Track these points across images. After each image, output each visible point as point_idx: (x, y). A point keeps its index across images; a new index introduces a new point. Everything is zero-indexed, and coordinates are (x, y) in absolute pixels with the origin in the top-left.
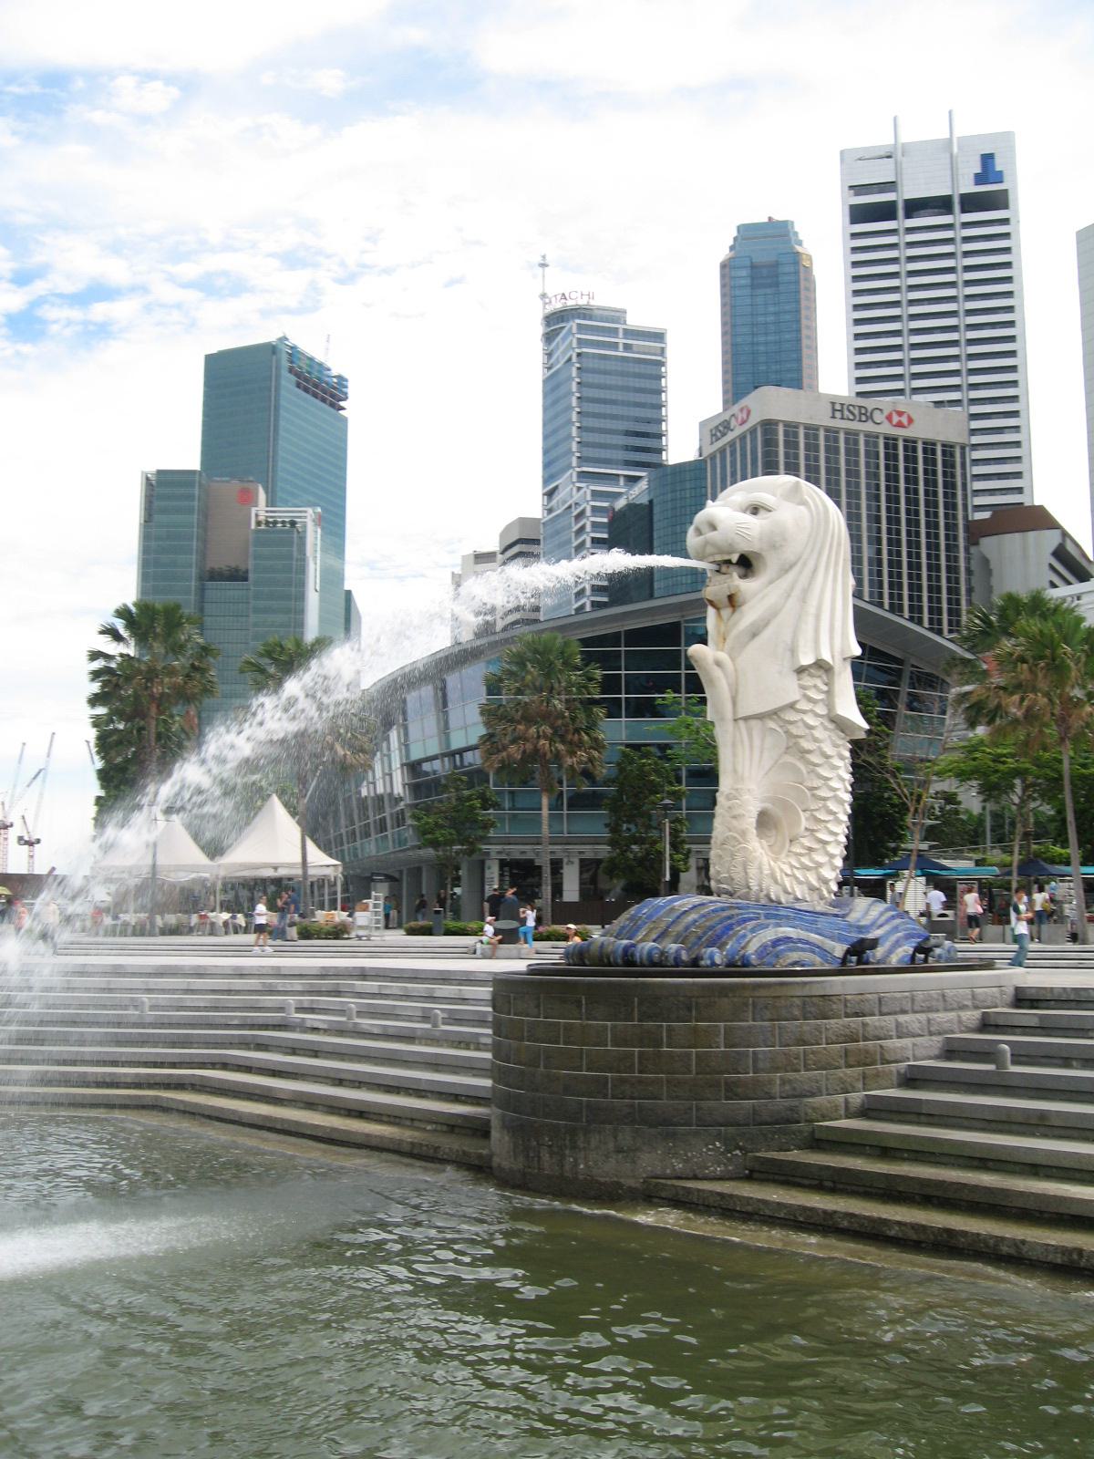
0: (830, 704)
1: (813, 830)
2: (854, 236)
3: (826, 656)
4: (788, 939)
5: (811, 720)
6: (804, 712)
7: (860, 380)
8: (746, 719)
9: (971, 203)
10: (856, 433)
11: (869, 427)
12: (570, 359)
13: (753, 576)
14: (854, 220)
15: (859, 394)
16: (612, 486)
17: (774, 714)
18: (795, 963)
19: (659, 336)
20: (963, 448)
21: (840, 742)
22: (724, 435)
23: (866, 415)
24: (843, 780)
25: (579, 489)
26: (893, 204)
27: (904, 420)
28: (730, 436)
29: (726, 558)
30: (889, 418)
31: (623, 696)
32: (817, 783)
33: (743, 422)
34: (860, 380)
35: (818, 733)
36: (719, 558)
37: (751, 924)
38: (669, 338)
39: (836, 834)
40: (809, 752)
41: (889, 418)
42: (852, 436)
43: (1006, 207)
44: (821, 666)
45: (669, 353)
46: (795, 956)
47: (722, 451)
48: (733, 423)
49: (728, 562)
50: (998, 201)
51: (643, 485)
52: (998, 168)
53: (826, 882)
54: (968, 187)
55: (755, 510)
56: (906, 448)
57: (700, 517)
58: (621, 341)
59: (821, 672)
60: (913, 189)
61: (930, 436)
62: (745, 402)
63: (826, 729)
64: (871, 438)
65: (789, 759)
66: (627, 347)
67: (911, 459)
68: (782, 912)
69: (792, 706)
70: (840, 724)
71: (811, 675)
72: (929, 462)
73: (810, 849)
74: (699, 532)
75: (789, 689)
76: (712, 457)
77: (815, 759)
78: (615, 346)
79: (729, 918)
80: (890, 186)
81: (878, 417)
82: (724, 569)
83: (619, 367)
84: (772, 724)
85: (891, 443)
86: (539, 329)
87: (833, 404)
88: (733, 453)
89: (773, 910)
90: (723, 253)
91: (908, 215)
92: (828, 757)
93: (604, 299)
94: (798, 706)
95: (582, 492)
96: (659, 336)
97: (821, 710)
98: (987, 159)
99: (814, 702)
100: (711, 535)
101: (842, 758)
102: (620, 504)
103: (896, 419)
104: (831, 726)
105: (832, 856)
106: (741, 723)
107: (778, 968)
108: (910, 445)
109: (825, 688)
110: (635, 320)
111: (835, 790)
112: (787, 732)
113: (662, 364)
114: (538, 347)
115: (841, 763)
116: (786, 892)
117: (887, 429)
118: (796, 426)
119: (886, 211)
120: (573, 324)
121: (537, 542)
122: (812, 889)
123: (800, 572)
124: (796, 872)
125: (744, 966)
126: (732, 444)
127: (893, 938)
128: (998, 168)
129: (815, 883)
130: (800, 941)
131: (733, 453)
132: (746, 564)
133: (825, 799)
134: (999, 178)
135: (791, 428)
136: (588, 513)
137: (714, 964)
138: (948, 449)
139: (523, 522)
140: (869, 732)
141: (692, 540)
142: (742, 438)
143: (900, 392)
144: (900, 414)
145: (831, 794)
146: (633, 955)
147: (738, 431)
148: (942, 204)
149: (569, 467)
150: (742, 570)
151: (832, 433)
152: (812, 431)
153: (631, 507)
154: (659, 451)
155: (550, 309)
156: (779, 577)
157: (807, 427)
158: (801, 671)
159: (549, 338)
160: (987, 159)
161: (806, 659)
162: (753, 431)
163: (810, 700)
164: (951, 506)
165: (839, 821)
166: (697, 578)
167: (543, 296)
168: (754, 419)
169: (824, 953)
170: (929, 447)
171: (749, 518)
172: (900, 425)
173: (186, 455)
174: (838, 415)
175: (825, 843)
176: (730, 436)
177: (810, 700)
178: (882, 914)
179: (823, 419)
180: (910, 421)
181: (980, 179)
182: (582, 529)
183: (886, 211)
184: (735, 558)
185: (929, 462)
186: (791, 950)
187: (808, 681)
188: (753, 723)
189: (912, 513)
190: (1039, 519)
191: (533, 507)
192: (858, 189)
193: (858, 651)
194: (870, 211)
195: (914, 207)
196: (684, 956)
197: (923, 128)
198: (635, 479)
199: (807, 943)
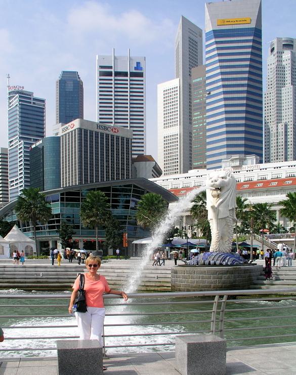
9: (133, 74)
11: (107, 132)
14: (100, 76)
15: (100, 122)
19: (43, 101)
20: (131, 139)
23: (106, 128)
25: (20, 141)
30: (112, 130)
33: (72, 128)
34: (100, 118)
38: (46, 102)
41: (112, 130)
42: (102, 134)
45: (46, 106)
47: (66, 135)
48: (69, 127)
50: (141, 75)
51: (41, 142)
56: (121, 139)
58: (32, 101)
62: (72, 122)
66: (34, 103)
72: (122, 143)
76: (62, 136)
78: (30, 103)
80: (111, 67)
85: (112, 136)
88: (69, 136)
90: (57, 77)
95: (21, 142)
98: (138, 64)
102: (33, 146)
108: (118, 138)
110: (36, 96)
113: (43, 109)
117: (111, 133)
119: (110, 74)
126: (69, 133)
131: (69, 136)
134: (141, 69)
135: (86, 131)
138: (128, 140)
142: (72, 132)
144: (115, 129)
147: (70, 130)
148: (125, 74)
151: (97, 133)
152: (91, 132)
153: (36, 147)
160: (138, 64)
162: (75, 130)
164: (127, 153)
170: (123, 139)
172: (115, 132)
180: (118, 131)
181: (136, 68)
183: (110, 74)
185: (122, 143)
190: (149, 159)
192: (101, 67)
194: (105, 73)
195: (117, 74)
198: (37, 140)
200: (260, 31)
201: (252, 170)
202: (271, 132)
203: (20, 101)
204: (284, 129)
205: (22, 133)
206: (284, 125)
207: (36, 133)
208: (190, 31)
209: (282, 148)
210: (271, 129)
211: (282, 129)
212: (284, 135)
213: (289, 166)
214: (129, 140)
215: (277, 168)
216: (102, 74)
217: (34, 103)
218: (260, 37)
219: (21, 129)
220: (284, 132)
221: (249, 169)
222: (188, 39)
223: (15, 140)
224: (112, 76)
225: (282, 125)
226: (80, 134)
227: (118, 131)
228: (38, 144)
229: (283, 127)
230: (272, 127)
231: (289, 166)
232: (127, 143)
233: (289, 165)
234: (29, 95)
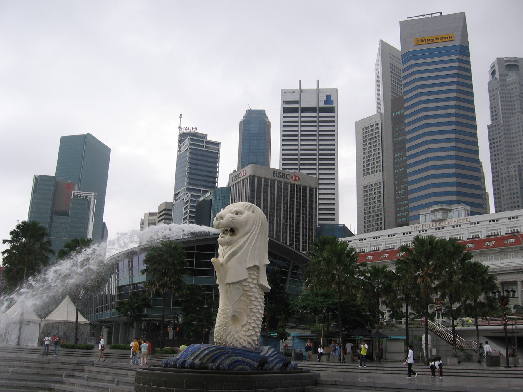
0: (258, 281)
1: (250, 323)
2: (284, 117)
3: (257, 263)
4: (238, 361)
5: (252, 286)
6: (250, 282)
7: (283, 164)
8: (229, 284)
9: (322, 110)
10: (281, 182)
11: (285, 180)
12: (187, 149)
13: (235, 235)
14: (284, 113)
16: (198, 193)
17: (239, 282)
18: (241, 369)
19: (218, 144)
21: (261, 293)
22: (237, 179)
23: (285, 176)
24: (262, 306)
25: (187, 193)
26: (298, 108)
27: (297, 179)
28: (239, 180)
29: (226, 229)
30: (292, 178)
31: (194, 268)
32: (253, 307)
34: (283, 164)
35: (255, 290)
36: (223, 229)
37: (226, 356)
38: (221, 145)
39: (258, 325)
40: (250, 296)
41: (292, 178)
42: (279, 183)
43: (334, 112)
44: (256, 267)
46: (240, 367)
47: (236, 184)
49: (227, 230)
50: (332, 110)
51: (209, 194)
52: (332, 100)
53: (254, 341)
54: (322, 105)
55: (237, 213)
57: (218, 214)
58: (205, 145)
59: (255, 269)
60: (305, 104)
61: (306, 184)
62: (245, 169)
63: (256, 288)
64: (286, 184)
65: (243, 298)
66: (207, 147)
67: (298, 191)
68: (238, 351)
69: (245, 280)
70: (262, 287)
71: (252, 270)
73: (249, 329)
74: (217, 219)
75: (244, 275)
76: (233, 186)
77: (253, 299)
78: (203, 146)
79: (219, 352)
80: (297, 102)
81: (288, 177)
82: (225, 232)
83: (203, 153)
84: (238, 286)
85: (292, 186)
86: (177, 139)
87: (274, 172)
89: (235, 351)
90: (241, 117)
91: (302, 112)
92: (257, 298)
93: (200, 131)
94: (248, 280)
96: (218, 144)
97: (255, 282)
98: (328, 97)
99: (253, 279)
100: (221, 221)
101: (262, 299)
102: (201, 199)
103: (294, 178)
104: (258, 287)
105: (256, 332)
106: (227, 285)
107: (235, 371)
108: (299, 187)
109: (257, 275)
110: (210, 138)
111: (259, 309)
112: (244, 290)
114: (176, 144)
115: (261, 300)
116: (240, 344)
118: (261, 178)
119: (295, 110)
120: (188, 139)
121: (171, 210)
122: (249, 343)
123: (250, 235)
124: (244, 337)
125: (223, 370)
126: (240, 182)
127: (276, 361)
128: (332, 100)
129: (251, 341)
130: (243, 361)
132: (232, 231)
133: (255, 312)
134: (332, 103)
135: (260, 179)
136: (189, 202)
137: (212, 369)
138: (311, 189)
139: (167, 203)
140: (270, 290)
141: (215, 222)
142: (243, 180)
143: (297, 169)
144: (296, 176)
145: (256, 311)
146: (185, 364)
147: (242, 178)
148: (313, 109)
149: (184, 185)
150: (231, 233)
151: (273, 181)
152: (266, 180)
154: (215, 182)
155: (181, 132)
156: (243, 237)
157: (265, 179)
158: (249, 268)
159: (180, 142)
160: (328, 97)
161: (251, 265)
162: (247, 178)
163: (252, 278)
165: (260, 320)
166: (215, 237)
167: (180, 128)
168: (248, 174)
169: (251, 366)
170: (305, 188)
171: (234, 216)
173: (51, 170)
174: (275, 175)
175: (254, 327)
176: (239, 180)
177: (252, 278)
178: (272, 352)
179: (270, 176)
180: (299, 179)
181: (325, 103)
182: (187, 206)
183: (295, 110)
184: (229, 229)
186: (240, 365)
187: (251, 272)
188: (231, 286)
189: (298, 209)
191: (171, 200)
192: (286, 102)
193: (268, 262)
194: (290, 109)
195: (305, 110)
196: (202, 366)
197: (309, 85)
199: (246, 362)
200: (467, 48)
201: (460, 226)
202: (501, 176)
203: (191, 144)
204: (517, 171)
205: (189, 184)
206: (516, 166)
207: (202, 183)
208: (392, 57)
209: (518, 197)
210: (500, 172)
211: (515, 171)
212: (518, 179)
213: (510, 218)
214: (312, 191)
215: (494, 221)
216: (286, 110)
217: (207, 147)
218: (467, 54)
219: (189, 178)
220: (517, 175)
221: (456, 224)
222: (389, 66)
223: (182, 191)
224: (298, 112)
225: (515, 166)
226: (252, 183)
227: (299, 179)
228: (206, 196)
229: (516, 168)
230: (501, 170)
231: (510, 218)
232: (311, 194)
233: (509, 216)
234: (202, 138)
